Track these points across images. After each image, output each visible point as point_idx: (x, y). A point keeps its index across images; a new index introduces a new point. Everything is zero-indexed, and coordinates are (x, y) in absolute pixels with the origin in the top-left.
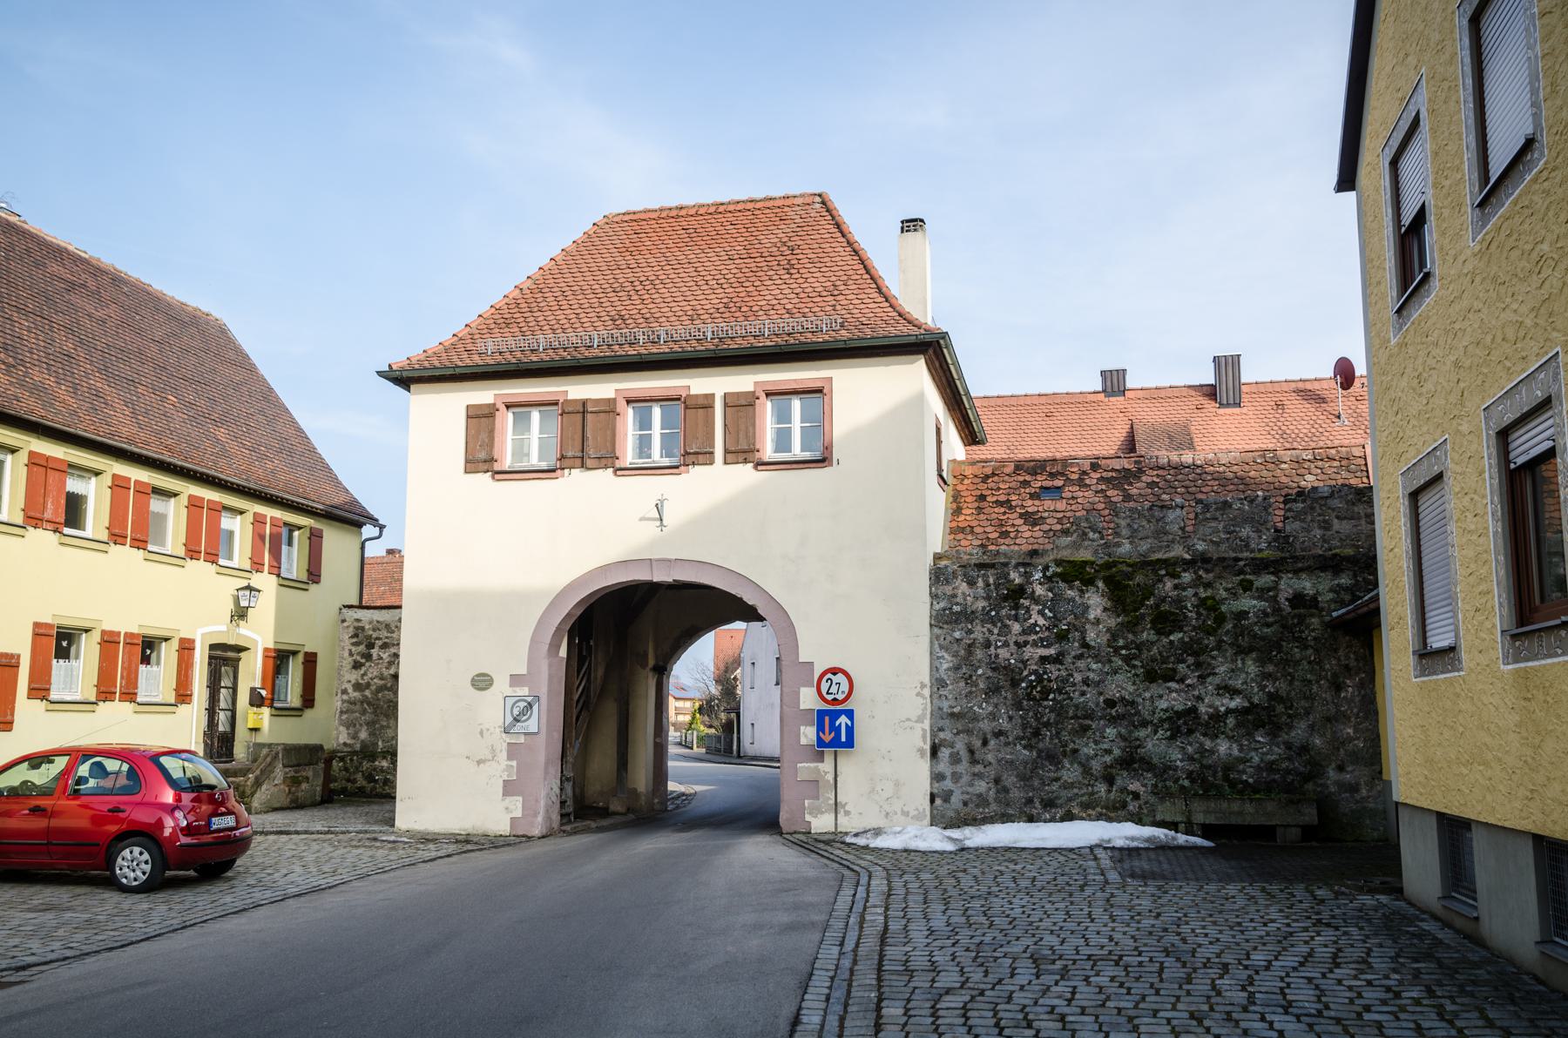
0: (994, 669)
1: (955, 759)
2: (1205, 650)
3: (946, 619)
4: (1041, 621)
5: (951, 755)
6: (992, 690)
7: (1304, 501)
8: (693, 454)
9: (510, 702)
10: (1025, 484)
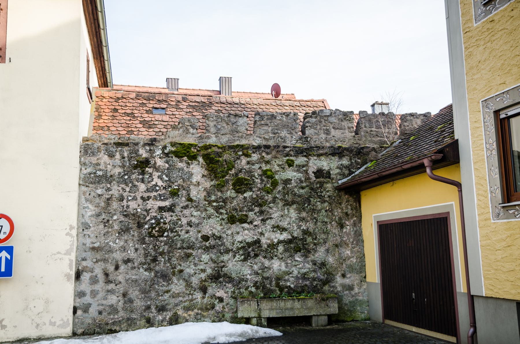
0: (125, 216)
1: (94, 281)
2: (265, 203)
3: (93, 179)
4: (160, 183)
5: (91, 278)
6: (125, 230)
7: (316, 117)
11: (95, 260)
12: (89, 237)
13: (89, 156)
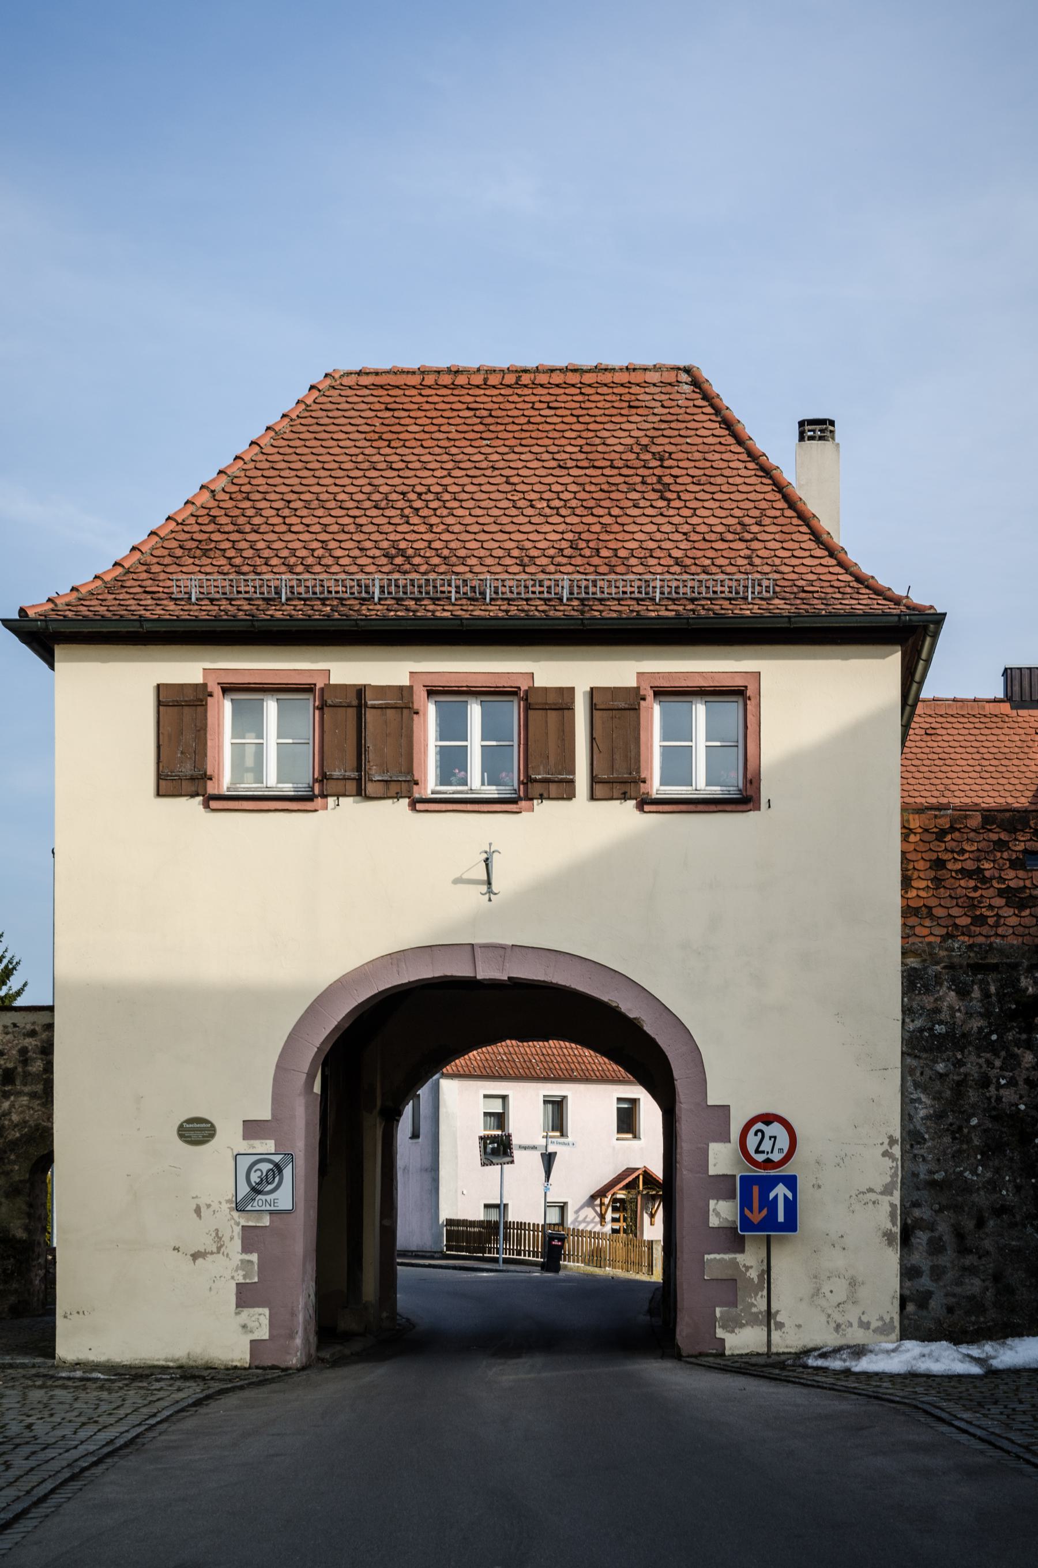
0: (994, 1119)
1: (936, 1247)
5: (930, 1241)
6: (992, 1149)
8: (540, 780)
9: (245, 1163)
10: (1001, 845)
11: (937, 1207)
12: (924, 1159)
13: (920, 994)
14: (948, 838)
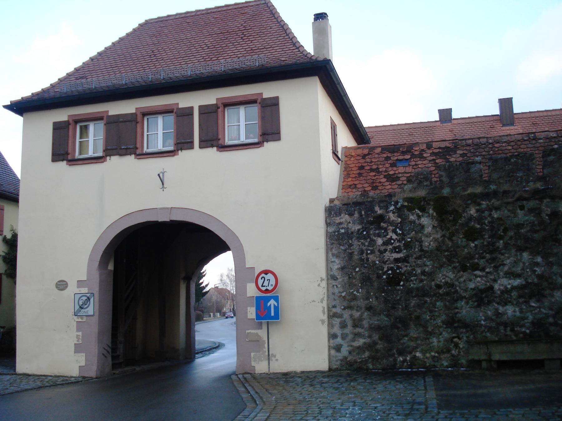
1: (343, 326)
2: (497, 250)
4: (394, 237)
5: (340, 323)
7: (554, 155)
8: (183, 143)
9: (78, 297)
10: (387, 158)
11: (343, 307)
12: (337, 287)
13: (333, 217)
14: (367, 157)
